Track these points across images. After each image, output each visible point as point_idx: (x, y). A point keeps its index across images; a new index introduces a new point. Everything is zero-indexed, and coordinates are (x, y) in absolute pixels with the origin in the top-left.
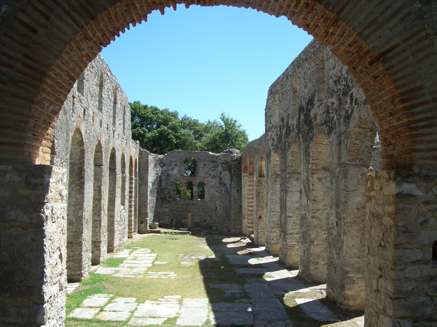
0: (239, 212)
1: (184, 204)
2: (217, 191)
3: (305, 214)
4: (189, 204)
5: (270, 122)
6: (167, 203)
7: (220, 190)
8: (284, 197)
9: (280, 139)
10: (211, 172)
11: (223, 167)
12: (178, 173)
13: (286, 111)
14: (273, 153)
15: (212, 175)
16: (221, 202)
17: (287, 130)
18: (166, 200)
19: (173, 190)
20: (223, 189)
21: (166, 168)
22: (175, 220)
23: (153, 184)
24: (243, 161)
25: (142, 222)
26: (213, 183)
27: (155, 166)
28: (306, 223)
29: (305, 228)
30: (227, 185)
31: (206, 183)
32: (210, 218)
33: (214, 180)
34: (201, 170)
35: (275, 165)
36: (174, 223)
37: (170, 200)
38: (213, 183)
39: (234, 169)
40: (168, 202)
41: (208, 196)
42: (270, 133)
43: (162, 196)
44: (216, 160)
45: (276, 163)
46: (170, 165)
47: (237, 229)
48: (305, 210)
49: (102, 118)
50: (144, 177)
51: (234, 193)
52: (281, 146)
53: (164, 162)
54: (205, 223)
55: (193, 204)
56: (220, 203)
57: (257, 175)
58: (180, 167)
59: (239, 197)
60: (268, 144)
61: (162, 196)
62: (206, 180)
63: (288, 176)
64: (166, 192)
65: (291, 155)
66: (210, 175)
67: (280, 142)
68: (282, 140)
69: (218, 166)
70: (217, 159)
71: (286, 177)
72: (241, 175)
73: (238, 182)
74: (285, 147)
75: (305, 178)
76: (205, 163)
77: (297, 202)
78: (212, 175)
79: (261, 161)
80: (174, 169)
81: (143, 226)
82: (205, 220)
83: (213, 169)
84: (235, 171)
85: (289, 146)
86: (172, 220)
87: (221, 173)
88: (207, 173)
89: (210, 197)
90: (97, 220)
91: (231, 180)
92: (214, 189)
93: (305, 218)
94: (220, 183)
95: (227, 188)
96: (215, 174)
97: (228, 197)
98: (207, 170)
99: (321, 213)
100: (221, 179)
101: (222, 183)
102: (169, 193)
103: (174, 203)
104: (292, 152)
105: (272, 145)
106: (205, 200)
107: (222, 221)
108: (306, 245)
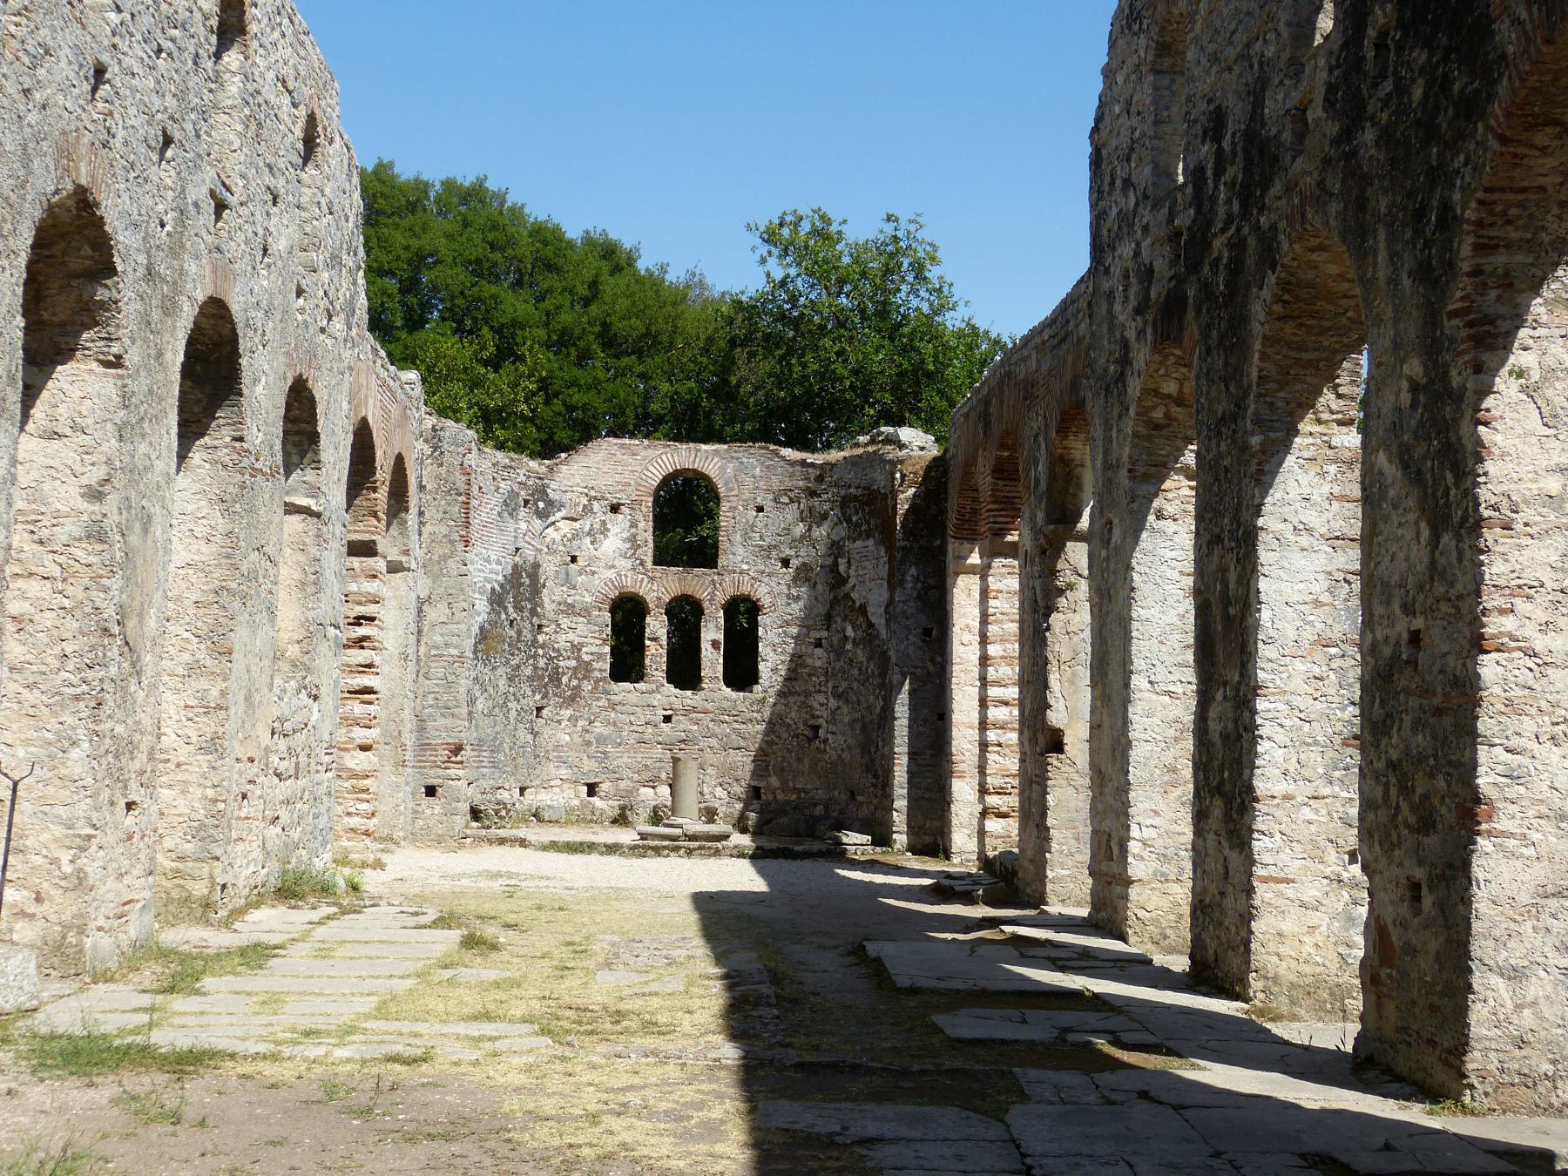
2: (818, 644)
3: (1415, 638)
5: (1127, 183)
7: (835, 639)
8: (1232, 576)
9: (1190, 248)
11: (849, 521)
13: (1244, 57)
14: (1141, 356)
15: (795, 563)
16: (838, 696)
17: (1246, 170)
20: (850, 632)
23: (496, 600)
24: (955, 478)
27: (510, 506)
28: (1426, 692)
29: (1418, 725)
30: (870, 610)
31: (766, 601)
35: (1157, 427)
40: (572, 699)
41: (775, 670)
42: (1126, 250)
43: (542, 663)
45: (1158, 414)
48: (1409, 610)
49: (105, 58)
50: (445, 558)
52: (1206, 288)
53: (552, 495)
56: (833, 703)
57: (1040, 516)
60: (1111, 316)
63: (1255, 440)
65: (1278, 308)
67: (1194, 266)
68: (1210, 244)
71: (1245, 447)
72: (943, 550)
74: (1236, 267)
75: (1406, 398)
77: (1317, 603)
78: (795, 563)
79: (1063, 431)
80: (604, 531)
83: (800, 529)
85: (1269, 257)
90: (77, 698)
91: (894, 581)
93: (1412, 663)
94: (835, 601)
95: (871, 625)
99: (1543, 617)
103: (603, 702)
104: (1284, 285)
105: (1138, 311)
106: (757, 688)
107: (844, 797)
108: (1432, 841)
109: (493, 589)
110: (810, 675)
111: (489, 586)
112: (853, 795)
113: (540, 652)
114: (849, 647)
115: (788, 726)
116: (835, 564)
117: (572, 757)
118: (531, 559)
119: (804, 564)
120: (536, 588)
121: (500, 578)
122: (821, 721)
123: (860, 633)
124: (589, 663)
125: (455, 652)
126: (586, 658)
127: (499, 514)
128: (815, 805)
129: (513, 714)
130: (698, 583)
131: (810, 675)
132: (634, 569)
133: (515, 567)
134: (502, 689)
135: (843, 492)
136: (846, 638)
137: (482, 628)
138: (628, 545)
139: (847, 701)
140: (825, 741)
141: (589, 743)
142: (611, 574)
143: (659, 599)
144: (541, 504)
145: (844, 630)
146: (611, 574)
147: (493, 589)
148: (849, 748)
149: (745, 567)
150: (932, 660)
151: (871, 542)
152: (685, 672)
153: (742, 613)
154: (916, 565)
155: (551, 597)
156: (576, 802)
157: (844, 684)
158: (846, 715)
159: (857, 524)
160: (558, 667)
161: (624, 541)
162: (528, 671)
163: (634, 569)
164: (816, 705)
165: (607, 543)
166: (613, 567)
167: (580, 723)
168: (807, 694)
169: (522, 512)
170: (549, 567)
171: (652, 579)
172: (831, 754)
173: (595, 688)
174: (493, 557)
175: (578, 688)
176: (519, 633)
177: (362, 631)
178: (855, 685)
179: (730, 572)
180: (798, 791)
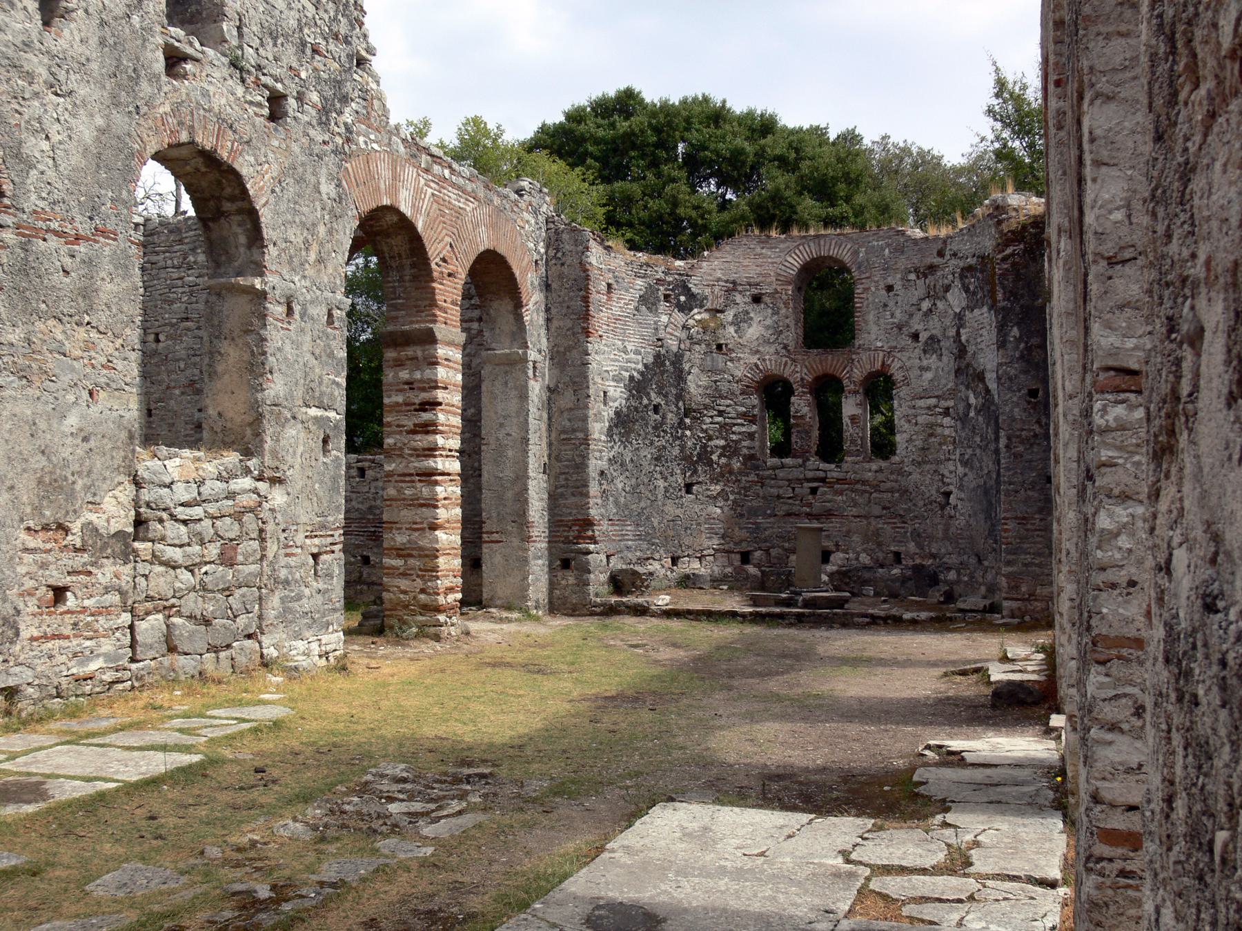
0: (1040, 511)
2: (946, 412)
4: (823, 480)
6: (715, 480)
7: (961, 407)
10: (916, 325)
11: (967, 290)
15: (923, 336)
16: (965, 463)
18: (710, 463)
19: (743, 415)
20: (972, 400)
21: (706, 316)
25: (566, 564)
26: (929, 375)
31: (898, 377)
32: (920, 546)
33: (932, 360)
34: (871, 317)
36: (751, 569)
38: (929, 375)
39: (1009, 283)
41: (910, 441)
44: (937, 260)
47: (1032, 596)
51: (1011, 406)
54: (896, 571)
55: (838, 481)
56: (961, 470)
58: (775, 313)
59: (1036, 428)
62: (896, 364)
66: (915, 337)
69: (947, 289)
70: (941, 254)
73: (1029, 349)
76: (890, 281)
78: (923, 336)
81: (572, 580)
82: (897, 555)
83: (926, 305)
84: (1012, 295)
87: (959, 317)
88: (900, 327)
89: (919, 443)
92: (933, 401)
94: (958, 372)
95: (988, 391)
96: (937, 332)
97: (991, 436)
98: (898, 313)
100: (962, 351)
101: (968, 374)
103: (752, 477)
106: (896, 459)
107: (973, 561)
109: (632, 378)
110: (940, 444)
111: (627, 375)
112: (980, 561)
113: (688, 433)
114: (972, 414)
115: (923, 494)
116: (958, 333)
118: (675, 349)
119: (932, 338)
120: (680, 376)
121: (640, 367)
122: (951, 488)
123: (980, 400)
124: (736, 442)
126: (734, 437)
127: (637, 309)
128: (949, 569)
129: (660, 493)
130: (830, 362)
131: (940, 444)
132: (777, 353)
133: (657, 356)
134: (647, 468)
135: (961, 264)
136: (969, 406)
137: (618, 413)
139: (972, 468)
140: (955, 507)
142: (754, 359)
143: (802, 379)
144: (683, 298)
145: (967, 398)
146: (754, 359)
147: (632, 378)
148: (975, 514)
149: (879, 344)
150: (1038, 422)
151: (985, 309)
152: (831, 448)
153: (879, 388)
154: (1018, 324)
155: (696, 384)
156: (729, 570)
157: (969, 451)
158: (972, 480)
159: (974, 293)
161: (767, 328)
162: (676, 451)
164: (946, 473)
165: (751, 331)
166: (757, 352)
167: (732, 497)
168: (939, 462)
169: (663, 306)
171: (794, 360)
172: (961, 521)
174: (629, 348)
175: (728, 465)
176: (664, 417)
177: (426, 416)
178: (978, 451)
179: (865, 350)
180: (934, 556)
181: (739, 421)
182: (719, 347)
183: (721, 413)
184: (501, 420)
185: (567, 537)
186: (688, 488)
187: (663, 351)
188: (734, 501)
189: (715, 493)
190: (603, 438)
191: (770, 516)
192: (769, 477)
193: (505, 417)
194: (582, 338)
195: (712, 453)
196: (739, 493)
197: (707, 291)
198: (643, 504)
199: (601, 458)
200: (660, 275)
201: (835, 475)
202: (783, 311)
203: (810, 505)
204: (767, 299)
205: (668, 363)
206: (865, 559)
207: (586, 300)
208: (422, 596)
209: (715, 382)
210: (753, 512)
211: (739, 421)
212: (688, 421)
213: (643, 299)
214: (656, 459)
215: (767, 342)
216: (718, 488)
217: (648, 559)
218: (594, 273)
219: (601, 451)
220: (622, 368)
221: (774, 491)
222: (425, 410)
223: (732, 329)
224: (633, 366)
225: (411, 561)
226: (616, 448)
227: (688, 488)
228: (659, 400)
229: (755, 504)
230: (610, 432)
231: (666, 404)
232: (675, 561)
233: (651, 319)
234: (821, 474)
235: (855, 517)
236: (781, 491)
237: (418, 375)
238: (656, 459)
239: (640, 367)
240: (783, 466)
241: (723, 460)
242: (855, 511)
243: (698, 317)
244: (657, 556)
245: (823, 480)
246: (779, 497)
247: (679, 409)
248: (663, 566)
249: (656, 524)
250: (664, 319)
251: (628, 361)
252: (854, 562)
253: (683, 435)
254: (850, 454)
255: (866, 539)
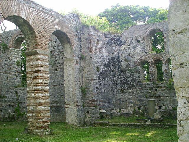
1: (152, 88)
4: (158, 87)
6: (130, 88)
12: (142, 52)
18: (128, 84)
22: (142, 107)
37: (133, 85)
40: (132, 87)
46: (131, 43)
53: (122, 40)
61: (122, 79)
64: (127, 74)
86: (139, 108)
102: (132, 75)
103: (140, 87)
109: (105, 63)
113: (122, 77)
117: (132, 101)
118: (117, 55)
120: (119, 62)
121: (108, 60)
124: (135, 78)
125: (90, 78)
126: (134, 77)
127: (106, 46)
129: (115, 92)
132: (144, 55)
133: (113, 58)
138: (142, 50)
141: (137, 97)
143: (151, 61)
144: (119, 43)
147: (105, 63)
160: (127, 80)
162: (119, 81)
163: (144, 55)
166: (139, 55)
167: (134, 93)
169: (113, 45)
170: (122, 58)
173: (137, 84)
174: (104, 56)
176: (115, 73)
177: (36, 75)
181: (135, 73)
182: (129, 54)
183: (131, 71)
184: (69, 76)
185: (88, 105)
186: (123, 91)
187: (114, 56)
188: (135, 94)
189: (130, 92)
190: (97, 79)
191: (145, 97)
192: (144, 87)
193: (69, 75)
194: (89, 53)
195: (129, 81)
196: (136, 92)
197: (125, 40)
198: (110, 96)
199: (96, 84)
200: (112, 37)
201: (161, 86)
202: (146, 44)
203: (155, 94)
204: (141, 41)
205: (115, 59)
206: (171, 108)
207: (90, 43)
208: (37, 124)
209: (129, 63)
210: (140, 96)
211: (135, 73)
212: (122, 74)
213: (108, 43)
214: (113, 84)
215: (142, 52)
216: (131, 90)
217: (113, 110)
218: (92, 37)
219: (96, 82)
220: (102, 61)
221: (146, 91)
222: (36, 73)
223: (133, 50)
224: (106, 60)
225: (34, 114)
226: (101, 81)
227: (123, 91)
228: (113, 69)
229: (141, 94)
230: (99, 77)
231: (116, 69)
232: (120, 110)
233: (110, 48)
234: (158, 86)
235: (167, 97)
236: (147, 91)
237: (34, 63)
238: (113, 84)
239: (108, 60)
240: (148, 84)
241: (132, 83)
242: (167, 95)
243: (123, 47)
244: (115, 109)
245: (158, 87)
246: (147, 92)
247: (119, 71)
248: (117, 112)
249: (114, 101)
250: (114, 48)
251: (104, 59)
252: (168, 109)
253: (121, 77)
254: (165, 80)
255: (170, 102)
